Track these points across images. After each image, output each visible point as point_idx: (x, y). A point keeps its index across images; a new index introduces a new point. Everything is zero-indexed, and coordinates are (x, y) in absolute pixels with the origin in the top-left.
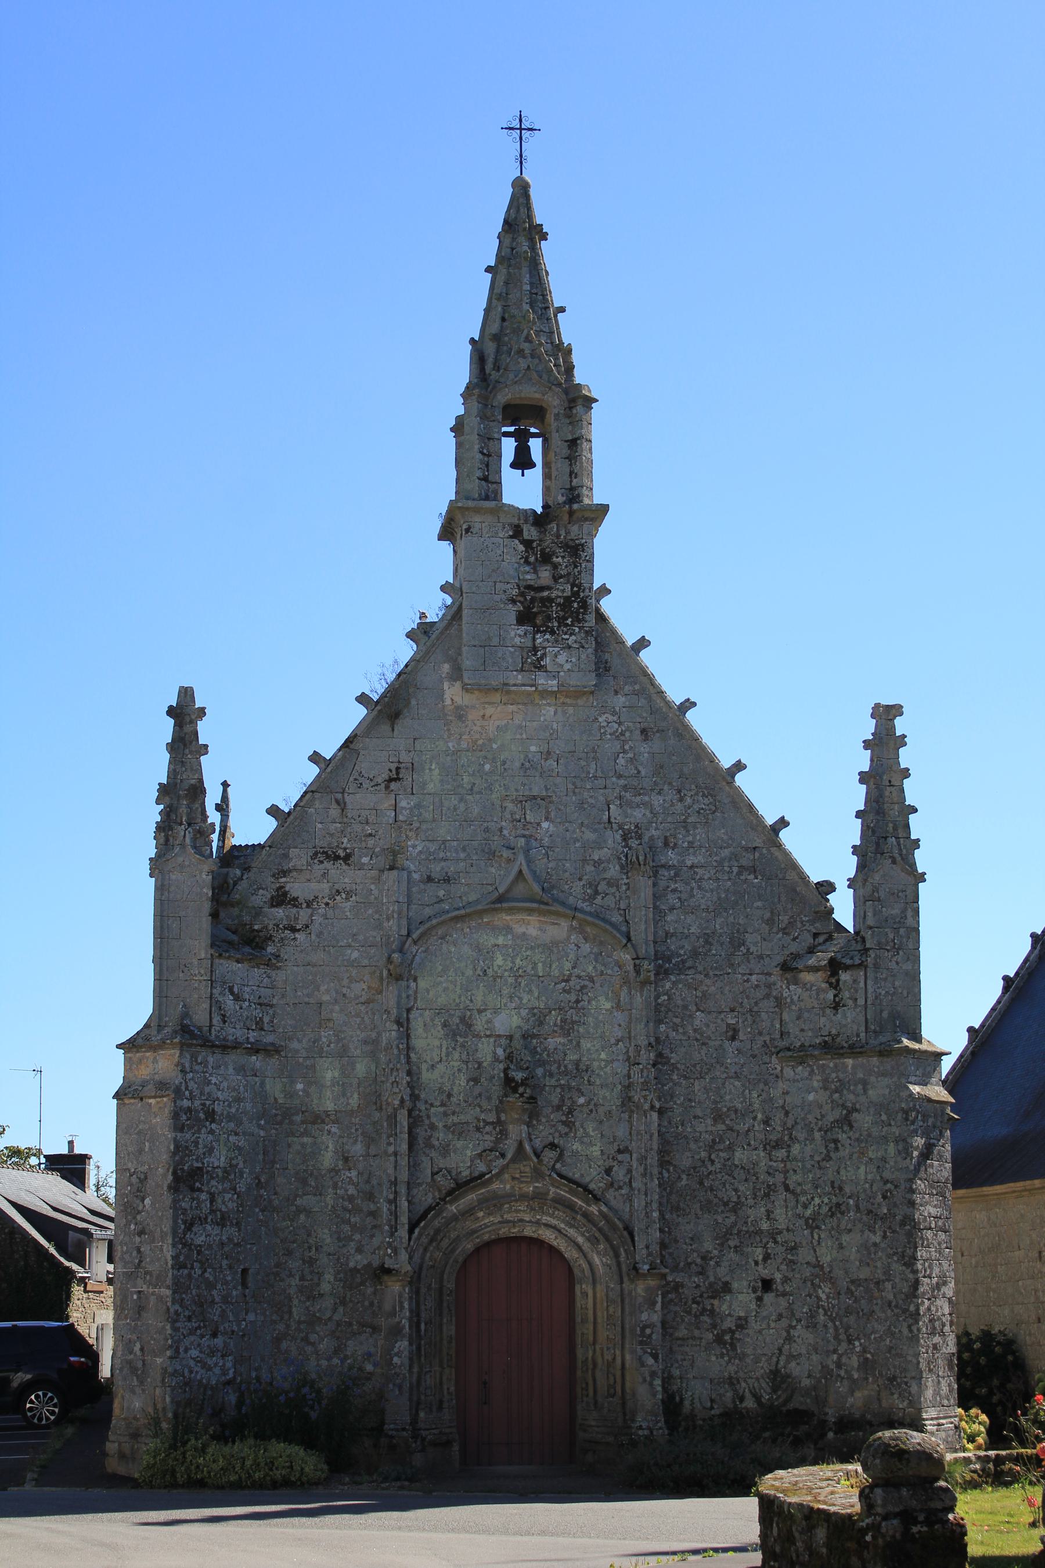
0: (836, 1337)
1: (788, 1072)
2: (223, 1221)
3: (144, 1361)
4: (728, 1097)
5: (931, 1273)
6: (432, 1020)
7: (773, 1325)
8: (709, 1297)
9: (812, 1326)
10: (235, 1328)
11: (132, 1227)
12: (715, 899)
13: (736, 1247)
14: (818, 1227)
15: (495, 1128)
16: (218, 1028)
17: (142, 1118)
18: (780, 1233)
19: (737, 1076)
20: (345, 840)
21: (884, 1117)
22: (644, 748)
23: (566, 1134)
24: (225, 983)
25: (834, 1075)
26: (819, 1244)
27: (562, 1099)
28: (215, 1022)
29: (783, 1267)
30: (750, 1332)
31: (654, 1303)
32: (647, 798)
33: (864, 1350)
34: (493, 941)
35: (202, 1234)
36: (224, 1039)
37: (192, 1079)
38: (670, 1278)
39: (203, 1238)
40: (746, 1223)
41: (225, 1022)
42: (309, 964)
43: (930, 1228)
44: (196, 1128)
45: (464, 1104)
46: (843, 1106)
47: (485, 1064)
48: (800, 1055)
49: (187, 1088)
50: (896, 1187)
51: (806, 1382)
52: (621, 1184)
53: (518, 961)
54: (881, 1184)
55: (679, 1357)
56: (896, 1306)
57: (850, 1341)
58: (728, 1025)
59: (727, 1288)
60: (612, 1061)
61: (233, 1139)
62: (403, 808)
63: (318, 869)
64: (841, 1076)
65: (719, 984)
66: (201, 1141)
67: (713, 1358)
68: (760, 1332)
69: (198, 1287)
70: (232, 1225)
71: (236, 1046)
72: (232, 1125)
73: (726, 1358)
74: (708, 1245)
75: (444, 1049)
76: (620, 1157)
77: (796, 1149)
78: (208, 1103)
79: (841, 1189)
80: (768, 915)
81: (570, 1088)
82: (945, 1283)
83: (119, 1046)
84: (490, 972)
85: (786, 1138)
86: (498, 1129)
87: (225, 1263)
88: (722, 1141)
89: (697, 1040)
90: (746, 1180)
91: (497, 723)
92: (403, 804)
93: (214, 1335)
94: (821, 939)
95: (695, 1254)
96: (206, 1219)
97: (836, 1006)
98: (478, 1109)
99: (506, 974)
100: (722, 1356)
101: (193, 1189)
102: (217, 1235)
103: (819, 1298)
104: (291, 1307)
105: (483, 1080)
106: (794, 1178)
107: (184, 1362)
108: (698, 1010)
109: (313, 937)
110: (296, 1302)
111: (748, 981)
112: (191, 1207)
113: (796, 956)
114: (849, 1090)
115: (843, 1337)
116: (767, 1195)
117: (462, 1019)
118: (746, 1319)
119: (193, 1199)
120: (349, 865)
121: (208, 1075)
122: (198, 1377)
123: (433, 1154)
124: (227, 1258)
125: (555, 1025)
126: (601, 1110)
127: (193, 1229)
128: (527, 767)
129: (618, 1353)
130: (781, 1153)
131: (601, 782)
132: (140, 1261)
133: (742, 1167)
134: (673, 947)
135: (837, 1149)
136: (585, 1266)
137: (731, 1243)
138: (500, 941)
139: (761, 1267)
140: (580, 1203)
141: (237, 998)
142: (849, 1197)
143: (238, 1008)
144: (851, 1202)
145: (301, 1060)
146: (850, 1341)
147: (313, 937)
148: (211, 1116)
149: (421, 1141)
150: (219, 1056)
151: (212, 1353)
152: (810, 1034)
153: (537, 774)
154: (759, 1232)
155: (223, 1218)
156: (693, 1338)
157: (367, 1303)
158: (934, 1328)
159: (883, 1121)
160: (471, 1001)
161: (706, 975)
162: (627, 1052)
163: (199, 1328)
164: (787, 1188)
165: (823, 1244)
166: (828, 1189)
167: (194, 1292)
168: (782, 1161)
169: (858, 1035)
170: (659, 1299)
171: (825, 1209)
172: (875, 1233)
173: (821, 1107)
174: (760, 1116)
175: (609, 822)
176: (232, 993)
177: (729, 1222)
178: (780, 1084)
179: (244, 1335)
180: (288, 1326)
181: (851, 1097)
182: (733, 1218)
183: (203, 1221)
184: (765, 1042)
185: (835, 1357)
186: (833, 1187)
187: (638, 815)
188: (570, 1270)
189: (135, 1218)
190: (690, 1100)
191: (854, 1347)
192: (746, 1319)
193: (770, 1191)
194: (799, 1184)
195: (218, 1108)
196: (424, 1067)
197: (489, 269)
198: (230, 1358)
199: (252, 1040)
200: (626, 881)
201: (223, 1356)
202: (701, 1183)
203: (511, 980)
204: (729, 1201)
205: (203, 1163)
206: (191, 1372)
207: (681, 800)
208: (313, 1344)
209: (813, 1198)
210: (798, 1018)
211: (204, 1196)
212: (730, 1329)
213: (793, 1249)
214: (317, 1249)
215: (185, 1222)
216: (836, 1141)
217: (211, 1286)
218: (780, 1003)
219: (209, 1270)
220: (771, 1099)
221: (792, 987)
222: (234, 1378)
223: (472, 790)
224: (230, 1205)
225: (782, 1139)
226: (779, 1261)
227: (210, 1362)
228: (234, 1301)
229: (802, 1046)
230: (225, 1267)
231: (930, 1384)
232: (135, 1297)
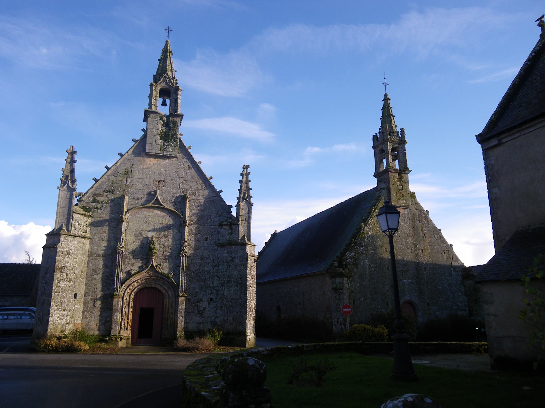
0: (227, 313)
1: (219, 249)
2: (70, 281)
3: (43, 318)
4: (204, 254)
5: (250, 297)
6: (132, 233)
7: (212, 309)
8: (197, 302)
9: (221, 309)
10: (71, 309)
11: (44, 282)
12: (204, 208)
13: (204, 290)
14: (224, 286)
15: (146, 260)
17: (49, 253)
18: (215, 287)
19: (207, 249)
20: (113, 188)
21: (241, 260)
22: (189, 171)
23: (164, 262)
24: (76, 220)
25: (230, 250)
26: (224, 289)
27: (163, 254)
28: (72, 229)
29: (215, 295)
30: (206, 311)
31: (183, 304)
32: (189, 183)
33: (234, 315)
34: (149, 214)
36: (75, 234)
37: (64, 243)
38: (187, 298)
40: (207, 285)
41: (75, 230)
42: (101, 217)
43: (251, 286)
44: (64, 256)
45: (138, 253)
46: (232, 257)
47: (145, 244)
48: (222, 245)
49: (62, 246)
50: (243, 276)
51: (219, 323)
52: (177, 274)
53: (155, 220)
54: (240, 276)
55: (189, 317)
56: (242, 305)
57: (230, 313)
58: (205, 237)
59: (201, 300)
60: (177, 245)
61: (75, 260)
62: (128, 181)
63: (105, 194)
64: (232, 250)
65: (204, 228)
66: (65, 260)
67: (197, 317)
68: (209, 311)
69: (60, 298)
70: (72, 282)
71: (78, 236)
72: (75, 256)
73: (200, 317)
74: (197, 290)
75: (134, 240)
76: (177, 268)
77: (220, 267)
78: (68, 250)
79: (230, 277)
80: (216, 212)
81: (166, 251)
82: (253, 300)
83: (45, 235)
84: (148, 222)
85: (218, 265)
86: (147, 260)
87: (69, 291)
88: (202, 265)
89: (198, 240)
90: (208, 274)
91: (153, 163)
92: (128, 180)
93: (64, 311)
94: (229, 219)
95: (194, 292)
96: (65, 280)
97: (231, 233)
98: (142, 255)
99: (152, 222)
100: (199, 317)
102: (67, 284)
103: (224, 303)
104: (88, 304)
105: (144, 248)
106: (219, 274)
107: (54, 318)
108: (198, 233)
109: (102, 211)
110: (90, 302)
111: (211, 227)
112: (60, 277)
113: (222, 222)
114: (233, 253)
115: (229, 312)
116: (212, 278)
117: (140, 233)
118: (206, 308)
119: (61, 275)
120: (113, 194)
121: (69, 243)
122: (58, 322)
123: (129, 265)
124: (70, 290)
125: (163, 235)
126: (173, 256)
128: (160, 173)
129: (173, 316)
130: (216, 268)
131: (178, 179)
132: (44, 291)
133: (207, 271)
134: (193, 218)
135: (230, 267)
136: (167, 294)
137: (203, 289)
138: (151, 214)
139: (210, 295)
140: (166, 279)
141: (79, 224)
142: (232, 279)
143: (79, 226)
144: (232, 280)
145: (96, 241)
146: (230, 313)
147: (102, 211)
148: (69, 253)
149: (127, 262)
150: (73, 238)
151: (63, 315)
152: (225, 240)
153: (163, 176)
154: (210, 287)
155: (70, 280)
156: (192, 312)
157: (109, 303)
158: (251, 310)
159: (241, 261)
160: (142, 228)
161: (201, 225)
162: (181, 243)
164: (217, 276)
165: (225, 290)
166: (227, 277)
167: (59, 299)
168: (217, 270)
169: (236, 240)
170: (184, 303)
171: (226, 281)
172: (238, 287)
173: (226, 257)
174: (212, 259)
175: (180, 188)
176: (78, 223)
177: (203, 284)
178: (217, 252)
179: (73, 311)
180: (87, 309)
181: (234, 255)
182: (204, 284)
183: (64, 281)
184: (214, 242)
185: (226, 317)
186: (228, 276)
187: (186, 187)
188: (163, 295)
189: (44, 279)
190: (195, 255)
191: (231, 315)
192: (206, 308)
193: (213, 277)
194: (220, 276)
195: (71, 252)
196: (129, 244)
197: (159, 60)
198: (69, 317)
199: (83, 235)
200: (183, 202)
201: (66, 316)
202: (197, 275)
203: (152, 224)
204: (203, 279)
205: (65, 265)
207: (197, 184)
208: (93, 313)
209: (223, 279)
210: (222, 236)
211: (64, 274)
212: (202, 310)
213: (218, 291)
214: (97, 289)
216: (229, 265)
217: (64, 298)
218: (218, 233)
219: (64, 293)
220: (215, 255)
221: (221, 229)
222: (70, 322)
223: (146, 178)
224: (73, 277)
225: (217, 265)
226: (215, 294)
227: (62, 318)
228: (71, 302)
229: (223, 243)
230: (69, 293)
231: (249, 324)
232: (42, 300)
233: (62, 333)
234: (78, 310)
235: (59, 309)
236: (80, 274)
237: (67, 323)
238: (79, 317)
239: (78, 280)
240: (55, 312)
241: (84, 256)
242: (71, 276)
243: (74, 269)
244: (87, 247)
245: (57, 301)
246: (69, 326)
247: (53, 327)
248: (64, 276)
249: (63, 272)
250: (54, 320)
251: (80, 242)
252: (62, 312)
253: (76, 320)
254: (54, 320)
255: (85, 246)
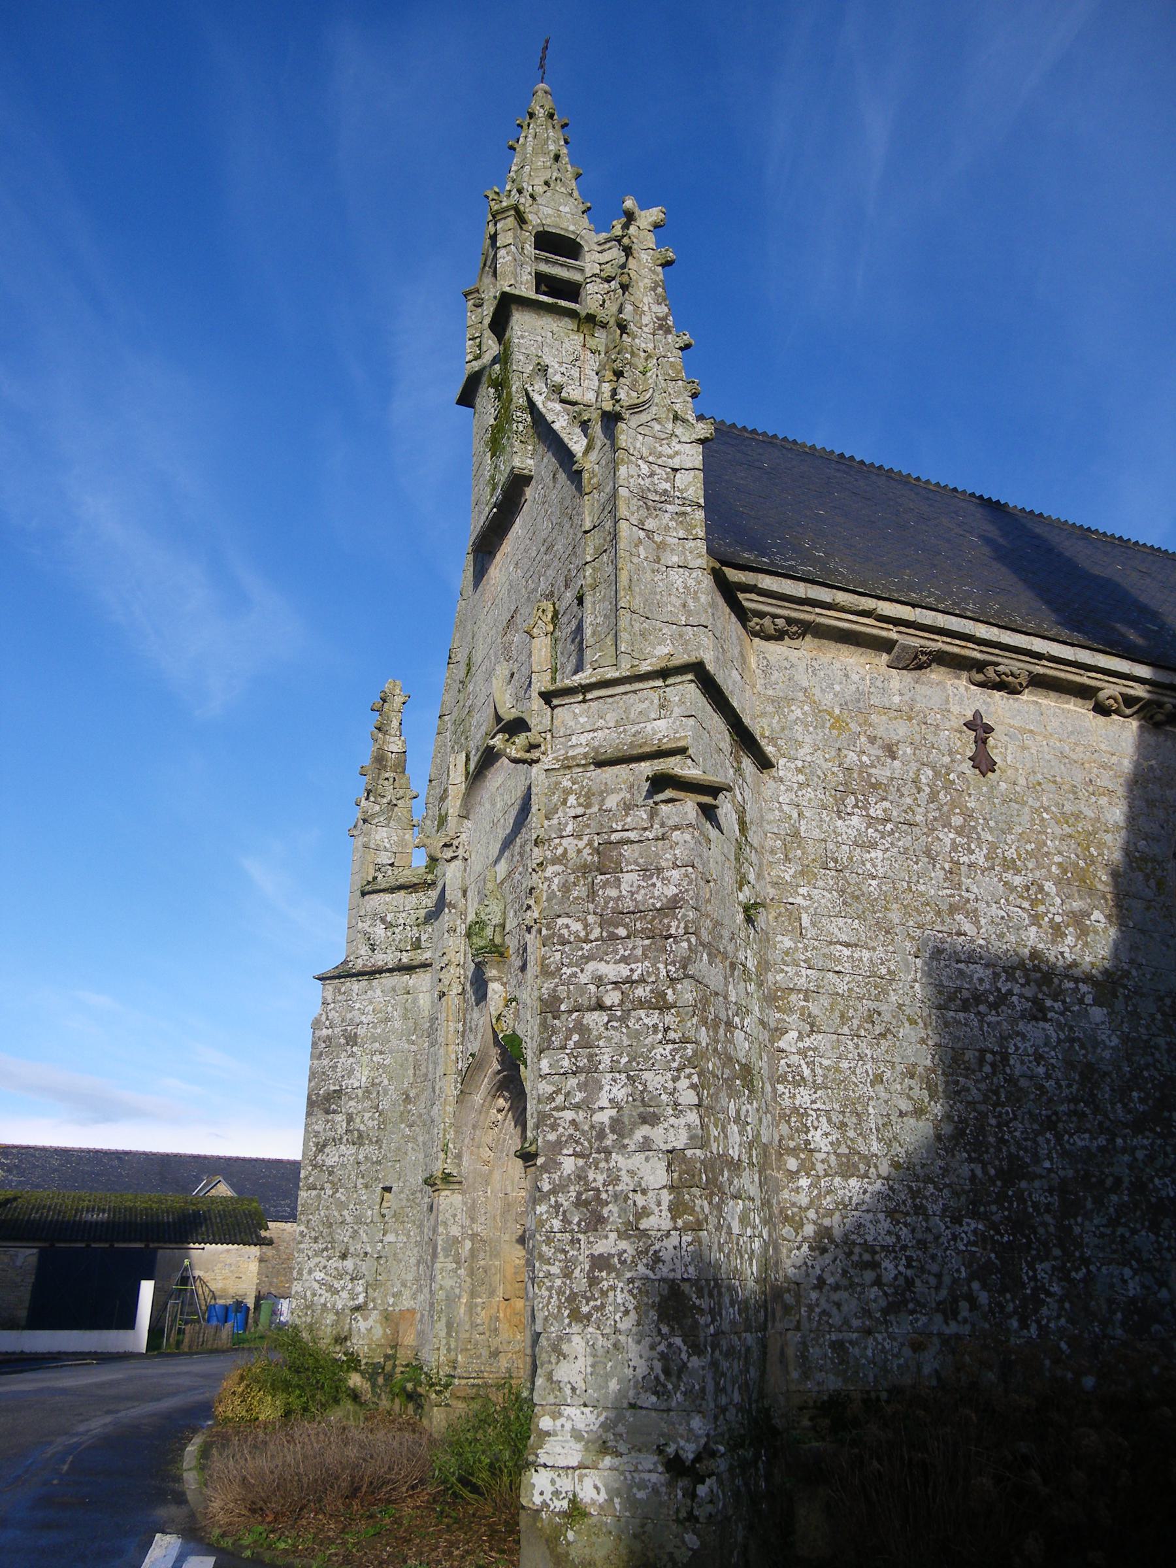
2: (359, 1140)
10: (369, 1250)
16: (365, 958)
35: (335, 1155)
37: (334, 1009)
39: (336, 1159)
41: (373, 950)
44: (334, 1054)
78: (349, 1028)
93: (344, 1257)
96: (341, 1138)
101: (327, 1112)
102: (352, 1155)
107: (307, 1284)
112: (325, 1129)
119: (328, 1121)
122: (322, 1301)
124: (363, 1177)
127: (326, 1150)
141: (389, 926)
143: (389, 934)
148: (352, 1040)
150: (366, 982)
151: (340, 1277)
155: (360, 1136)
163: (326, 1249)
167: (322, 1213)
183: (338, 1142)
195: (361, 1031)
198: (360, 1282)
205: (342, 1086)
206: (314, 1295)
211: (339, 1118)
215: (317, 1144)
217: (342, 1206)
219: (340, 1190)
222: (366, 1303)
224: (370, 1124)
227: (337, 1285)
228: (368, 1221)
233: (338, 1348)
234: (400, 1256)
235: (323, 1250)
236: (402, 1108)
237: (357, 1308)
238: (404, 1285)
239: (393, 1134)
240: (311, 1264)
241: (414, 1038)
242: (362, 1122)
243: (375, 1094)
244: (422, 1002)
245: (314, 1218)
246: (365, 1319)
247: (304, 1319)
248: (338, 1126)
249: (334, 1112)
250: (309, 1294)
251: (394, 990)
252: (335, 1263)
253: (394, 1296)
254: (309, 1294)
255: (415, 1000)
